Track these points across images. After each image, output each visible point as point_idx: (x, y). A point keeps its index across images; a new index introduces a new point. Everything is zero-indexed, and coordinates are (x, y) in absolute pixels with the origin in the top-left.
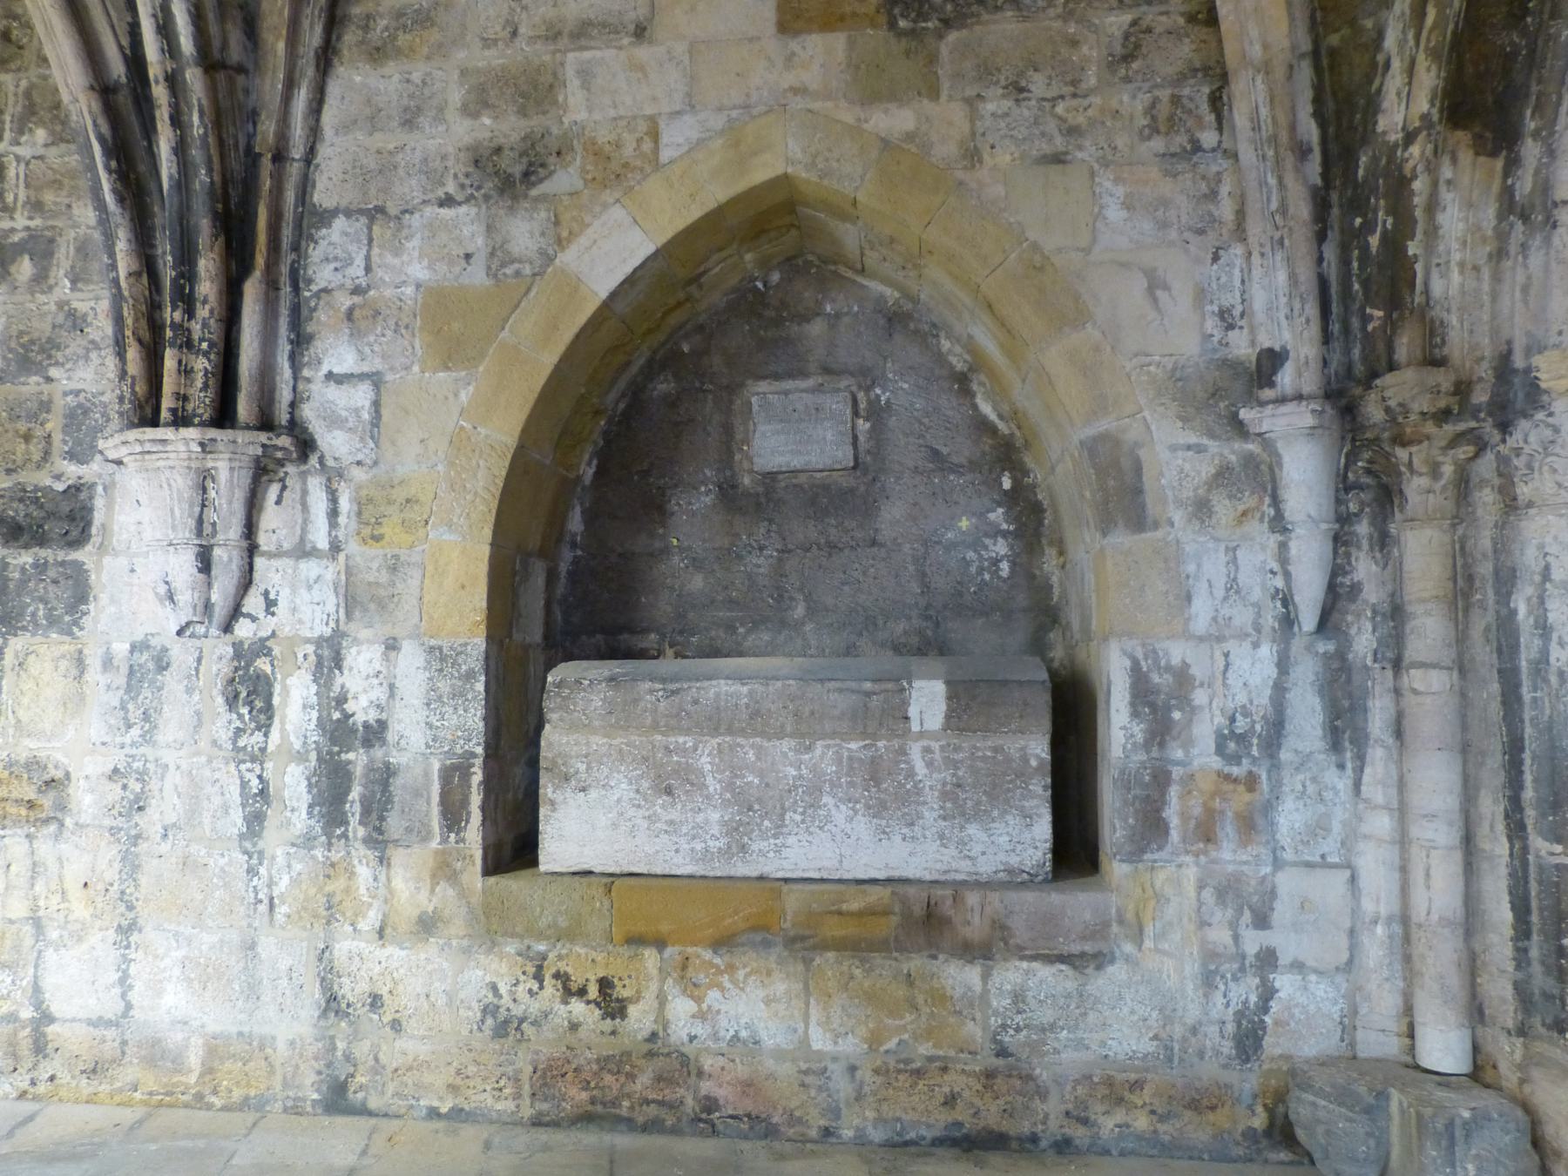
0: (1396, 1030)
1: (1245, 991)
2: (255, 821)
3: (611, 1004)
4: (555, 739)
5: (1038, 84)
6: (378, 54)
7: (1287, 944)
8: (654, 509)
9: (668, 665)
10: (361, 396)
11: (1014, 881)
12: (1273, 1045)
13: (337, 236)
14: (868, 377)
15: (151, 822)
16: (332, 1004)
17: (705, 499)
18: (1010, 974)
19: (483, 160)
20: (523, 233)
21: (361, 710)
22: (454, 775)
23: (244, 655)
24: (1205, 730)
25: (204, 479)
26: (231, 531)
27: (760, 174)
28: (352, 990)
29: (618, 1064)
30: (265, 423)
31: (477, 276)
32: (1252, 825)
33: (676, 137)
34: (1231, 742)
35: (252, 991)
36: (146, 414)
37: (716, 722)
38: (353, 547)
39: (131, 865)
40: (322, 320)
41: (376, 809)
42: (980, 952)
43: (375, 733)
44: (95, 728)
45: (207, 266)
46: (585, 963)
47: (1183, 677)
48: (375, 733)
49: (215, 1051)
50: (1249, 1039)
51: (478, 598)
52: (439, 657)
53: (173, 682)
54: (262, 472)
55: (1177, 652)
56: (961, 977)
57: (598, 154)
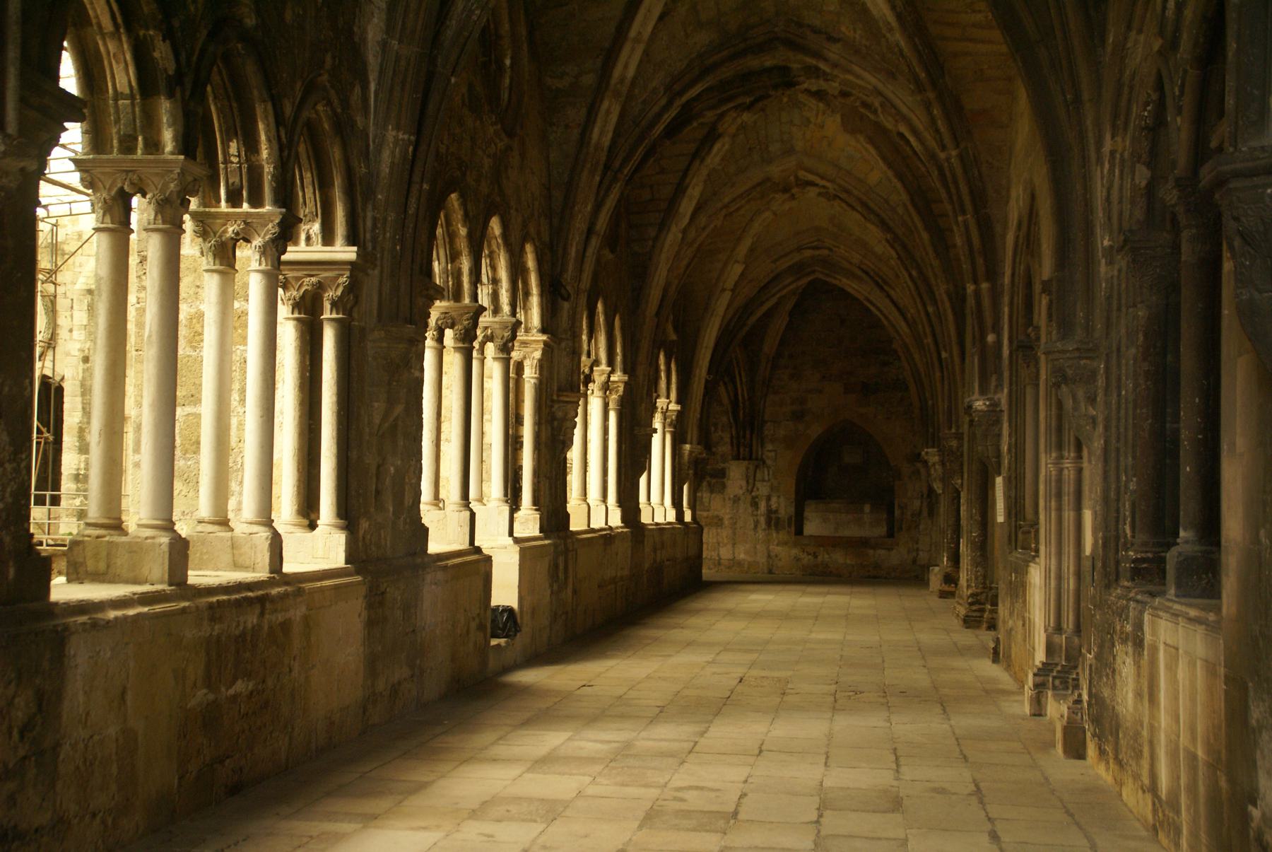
1: (915, 554)
2: (756, 527)
3: (816, 557)
4: (807, 514)
10: (773, 454)
16: (769, 556)
21: (774, 507)
22: (790, 519)
23: (753, 498)
25: (747, 469)
28: (772, 554)
30: (757, 459)
36: (737, 457)
39: (734, 534)
43: (776, 512)
45: (748, 432)
48: (776, 512)
50: (914, 561)
54: (757, 467)
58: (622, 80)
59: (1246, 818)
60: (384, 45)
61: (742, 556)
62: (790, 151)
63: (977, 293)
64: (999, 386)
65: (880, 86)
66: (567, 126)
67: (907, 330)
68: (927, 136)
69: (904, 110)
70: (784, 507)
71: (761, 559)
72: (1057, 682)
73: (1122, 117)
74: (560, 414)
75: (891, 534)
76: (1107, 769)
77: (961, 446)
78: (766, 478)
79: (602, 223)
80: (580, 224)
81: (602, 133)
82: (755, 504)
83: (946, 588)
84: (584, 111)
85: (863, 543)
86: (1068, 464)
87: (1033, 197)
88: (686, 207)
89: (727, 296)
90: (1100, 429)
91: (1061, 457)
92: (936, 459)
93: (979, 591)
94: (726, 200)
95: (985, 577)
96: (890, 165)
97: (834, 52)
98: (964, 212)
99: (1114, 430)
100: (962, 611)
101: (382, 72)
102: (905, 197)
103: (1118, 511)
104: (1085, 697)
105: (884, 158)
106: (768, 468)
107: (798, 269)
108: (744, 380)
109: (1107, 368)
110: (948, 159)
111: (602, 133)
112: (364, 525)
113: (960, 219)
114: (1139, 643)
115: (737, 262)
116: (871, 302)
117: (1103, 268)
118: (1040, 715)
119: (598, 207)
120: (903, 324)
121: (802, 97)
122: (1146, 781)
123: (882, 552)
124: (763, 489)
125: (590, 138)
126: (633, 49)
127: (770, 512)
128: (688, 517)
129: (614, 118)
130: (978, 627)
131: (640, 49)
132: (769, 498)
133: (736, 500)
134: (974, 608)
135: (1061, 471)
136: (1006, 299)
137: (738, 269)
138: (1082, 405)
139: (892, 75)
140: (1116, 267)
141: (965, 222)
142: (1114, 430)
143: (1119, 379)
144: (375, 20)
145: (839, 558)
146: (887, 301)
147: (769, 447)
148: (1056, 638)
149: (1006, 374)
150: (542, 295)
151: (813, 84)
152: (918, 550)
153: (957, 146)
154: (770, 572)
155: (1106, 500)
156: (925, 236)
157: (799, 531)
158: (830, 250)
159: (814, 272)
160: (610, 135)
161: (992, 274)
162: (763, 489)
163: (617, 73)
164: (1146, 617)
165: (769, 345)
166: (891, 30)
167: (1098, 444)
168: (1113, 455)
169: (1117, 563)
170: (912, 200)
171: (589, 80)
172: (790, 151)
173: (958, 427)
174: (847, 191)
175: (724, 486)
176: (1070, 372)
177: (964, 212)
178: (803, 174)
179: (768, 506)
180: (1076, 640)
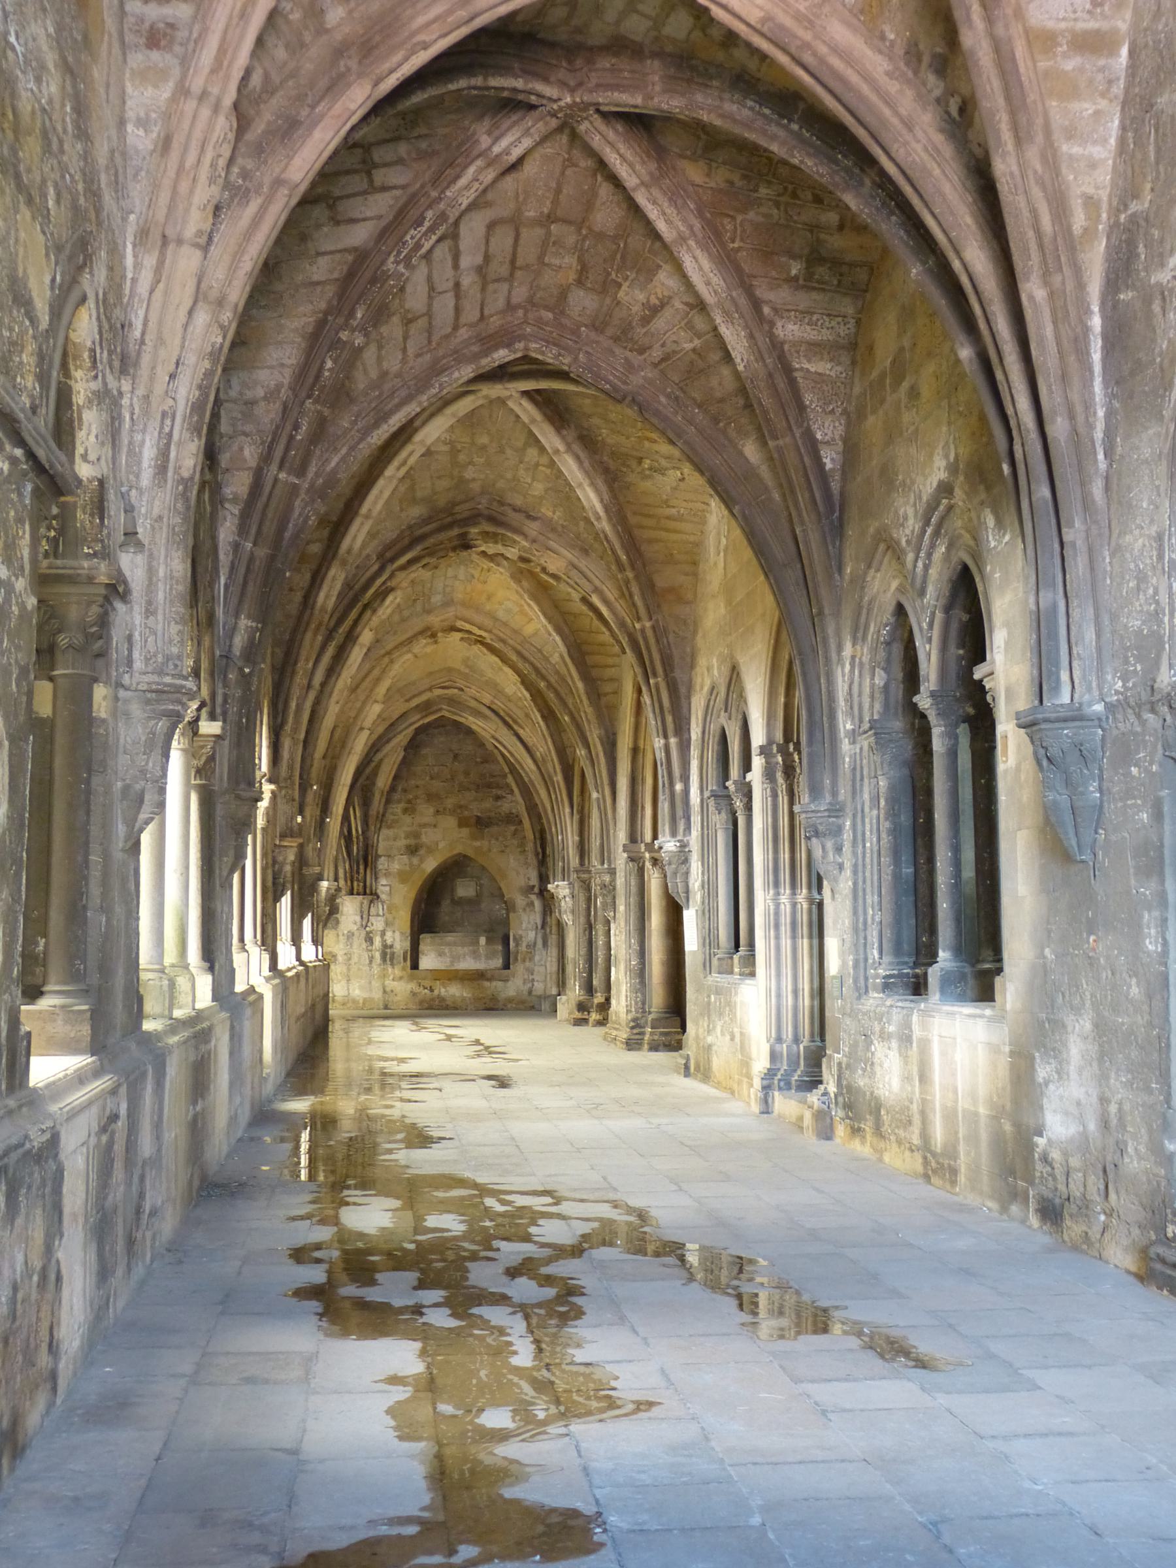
0: (1133, 1268)
1: (530, 985)
2: (371, 962)
3: (432, 990)
4: (422, 947)
5: (501, 839)
6: (389, 827)
7: (536, 977)
8: (438, 904)
9: (441, 934)
10: (388, 888)
11: (496, 969)
12: (534, 993)
13: (382, 860)
14: (479, 878)
15: (352, 962)
16: (385, 992)
17: (448, 901)
18: (494, 983)
19: (408, 847)
20: (415, 861)
21: (389, 942)
22: (405, 954)
23: (368, 933)
24: (524, 944)
25: (362, 903)
26: (366, 913)
27: (455, 852)
28: (388, 989)
29: (433, 1000)
30: (371, 894)
31: (407, 868)
32: (531, 959)
33: (441, 845)
34: (528, 946)
35: (371, 990)
36: (351, 893)
37: (449, 944)
38: (387, 915)
39: (349, 970)
40: (380, 874)
41: (392, 959)
42: (489, 980)
43: (391, 947)
44: (341, 946)
45: (362, 867)
46: (427, 983)
47: (521, 937)
48: (391, 947)
49: (365, 1000)
50: (530, 992)
51: (409, 924)
52: (402, 933)
53: (355, 938)
54: (371, 902)
55: (520, 932)
56: (487, 984)
57: (428, 848)
58: (349, 551)
59: (1030, 1147)
60: (236, 547)
61: (357, 992)
62: (448, 603)
63: (667, 748)
64: (688, 828)
65: (575, 561)
66: (291, 590)
67: (533, 767)
68: (621, 607)
69: (597, 583)
70: (399, 941)
71: (377, 995)
72: (782, 1084)
73: (861, 631)
74: (280, 858)
75: (507, 966)
76: (863, 1143)
77: (613, 880)
78: (381, 913)
80: (300, 679)
81: (327, 597)
82: (369, 939)
83: (578, 1015)
84: (308, 576)
85: (480, 976)
86: (785, 899)
89: (366, 733)
90: (848, 872)
91: (778, 894)
92: (567, 892)
93: (639, 1015)
94: (389, 647)
95: (644, 1003)
96: (550, 620)
97: (533, 528)
98: (655, 675)
99: (860, 874)
100: (624, 1035)
101: (233, 568)
102: (562, 648)
103: (865, 938)
104: (832, 1089)
105: (545, 615)
106: (383, 902)
107: (426, 707)
108: (358, 814)
109: (854, 826)
110: (643, 630)
111: (328, 596)
112: (217, 967)
113: (652, 681)
114: (906, 1039)
115: (376, 701)
116: (497, 740)
117: (845, 746)
118: (768, 1113)
120: (529, 761)
121: (475, 557)
122: (916, 1141)
123: (500, 984)
124: (378, 924)
125: (315, 602)
126: (362, 524)
127: (385, 946)
128: (320, 957)
129: (338, 586)
130: (639, 1049)
132: (383, 933)
133: (350, 935)
134: (635, 1031)
135: (777, 906)
136: (694, 753)
137: (377, 709)
138: (831, 854)
139: (585, 552)
140: (858, 746)
141: (657, 685)
142: (860, 874)
143: (864, 834)
144: (228, 524)
145: (454, 991)
146: (514, 739)
147: (383, 881)
148: (778, 1047)
149: (696, 819)
150: (269, 747)
151: (491, 548)
152: (533, 980)
153: (651, 619)
154: (386, 1007)
155: (855, 929)
156: (580, 685)
157: (415, 966)
158: (461, 690)
159: (441, 709)
160: (334, 599)
161: (682, 729)
162: (378, 924)
164: (915, 1018)
165: (383, 781)
166: (598, 518)
167: (845, 884)
168: (860, 894)
169: (866, 979)
170: (569, 652)
172: (448, 603)
173: (610, 863)
174: (503, 641)
175: (338, 922)
176: (820, 828)
177: (655, 675)
178: (460, 624)
179: (384, 942)
180: (795, 1046)
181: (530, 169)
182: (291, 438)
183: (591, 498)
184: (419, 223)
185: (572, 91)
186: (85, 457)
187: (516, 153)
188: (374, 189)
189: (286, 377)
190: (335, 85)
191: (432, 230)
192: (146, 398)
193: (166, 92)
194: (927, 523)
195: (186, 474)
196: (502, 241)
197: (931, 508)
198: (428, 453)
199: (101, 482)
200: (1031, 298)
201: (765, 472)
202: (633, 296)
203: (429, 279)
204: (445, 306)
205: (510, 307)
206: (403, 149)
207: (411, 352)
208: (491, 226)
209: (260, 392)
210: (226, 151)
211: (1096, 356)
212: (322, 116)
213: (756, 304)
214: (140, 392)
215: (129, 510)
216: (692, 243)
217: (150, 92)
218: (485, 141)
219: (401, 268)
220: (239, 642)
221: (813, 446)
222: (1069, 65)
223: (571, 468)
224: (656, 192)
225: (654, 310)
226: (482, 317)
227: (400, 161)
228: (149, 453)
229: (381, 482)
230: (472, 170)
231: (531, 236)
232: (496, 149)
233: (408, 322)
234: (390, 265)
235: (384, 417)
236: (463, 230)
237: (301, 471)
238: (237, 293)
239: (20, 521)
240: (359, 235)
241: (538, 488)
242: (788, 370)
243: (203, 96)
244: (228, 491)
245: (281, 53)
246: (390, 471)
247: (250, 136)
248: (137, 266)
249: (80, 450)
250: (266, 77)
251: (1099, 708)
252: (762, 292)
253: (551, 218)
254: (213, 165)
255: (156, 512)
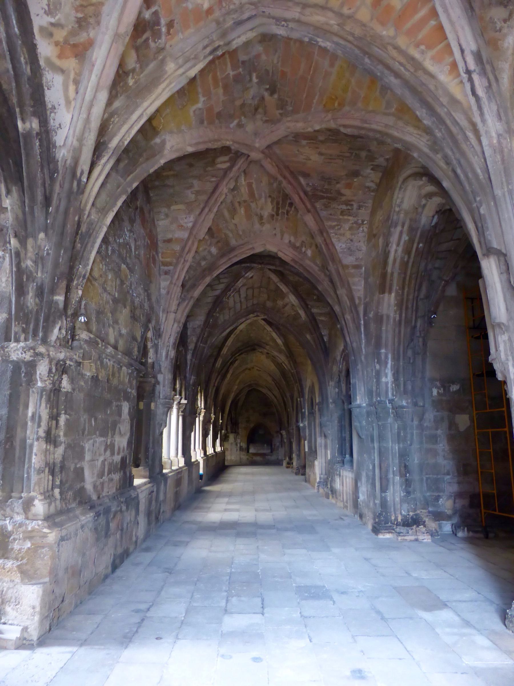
60: (191, 360)
79: (216, 385)
84: (213, 360)
87: (313, 383)
88: (229, 376)
97: (268, 347)
119: (216, 380)
129: (221, 362)
131: (227, 348)
163: (222, 353)
171: (215, 353)
181: (254, 278)
182: (203, 336)
183: (279, 341)
184: (230, 290)
185: (261, 264)
186: (150, 358)
187: (250, 276)
188: (220, 283)
189: (202, 323)
190: (203, 277)
191: (233, 292)
192: (164, 343)
193: (168, 283)
194: (341, 357)
195: (172, 357)
196: (250, 292)
197: (342, 354)
198: (241, 331)
199: (153, 363)
200: (347, 319)
201: (312, 342)
202: (280, 303)
203: (234, 300)
204: (238, 306)
205: (253, 305)
206: (226, 275)
207: (231, 315)
208: (247, 289)
209: (197, 326)
210: (180, 294)
211: (362, 329)
212: (201, 283)
213: (307, 305)
214: (162, 342)
215: (160, 366)
216: (290, 293)
217: (165, 283)
218: (244, 273)
219: (227, 300)
220: (191, 382)
221: (322, 336)
222: (352, 271)
223: (274, 335)
224: (282, 283)
225: (285, 306)
226: (247, 307)
227: (225, 278)
228: (164, 354)
229: (230, 339)
230: (240, 280)
231: (256, 291)
232: (246, 275)
233: (230, 309)
234: (224, 299)
235: (225, 330)
236: (241, 290)
237: (206, 343)
238: (183, 320)
239: (133, 380)
240: (217, 292)
241: (268, 338)
242: (315, 320)
243: (175, 284)
244: (190, 348)
245: (192, 272)
246: (232, 336)
247: (186, 288)
248: (162, 316)
249: (149, 357)
250: (189, 277)
251: (364, 405)
252: (308, 302)
253: (260, 287)
254: (177, 297)
255: (165, 366)
